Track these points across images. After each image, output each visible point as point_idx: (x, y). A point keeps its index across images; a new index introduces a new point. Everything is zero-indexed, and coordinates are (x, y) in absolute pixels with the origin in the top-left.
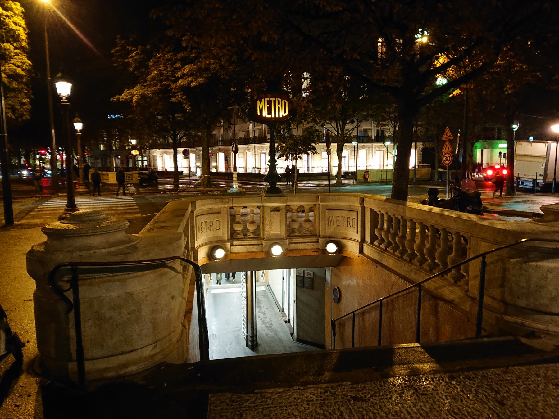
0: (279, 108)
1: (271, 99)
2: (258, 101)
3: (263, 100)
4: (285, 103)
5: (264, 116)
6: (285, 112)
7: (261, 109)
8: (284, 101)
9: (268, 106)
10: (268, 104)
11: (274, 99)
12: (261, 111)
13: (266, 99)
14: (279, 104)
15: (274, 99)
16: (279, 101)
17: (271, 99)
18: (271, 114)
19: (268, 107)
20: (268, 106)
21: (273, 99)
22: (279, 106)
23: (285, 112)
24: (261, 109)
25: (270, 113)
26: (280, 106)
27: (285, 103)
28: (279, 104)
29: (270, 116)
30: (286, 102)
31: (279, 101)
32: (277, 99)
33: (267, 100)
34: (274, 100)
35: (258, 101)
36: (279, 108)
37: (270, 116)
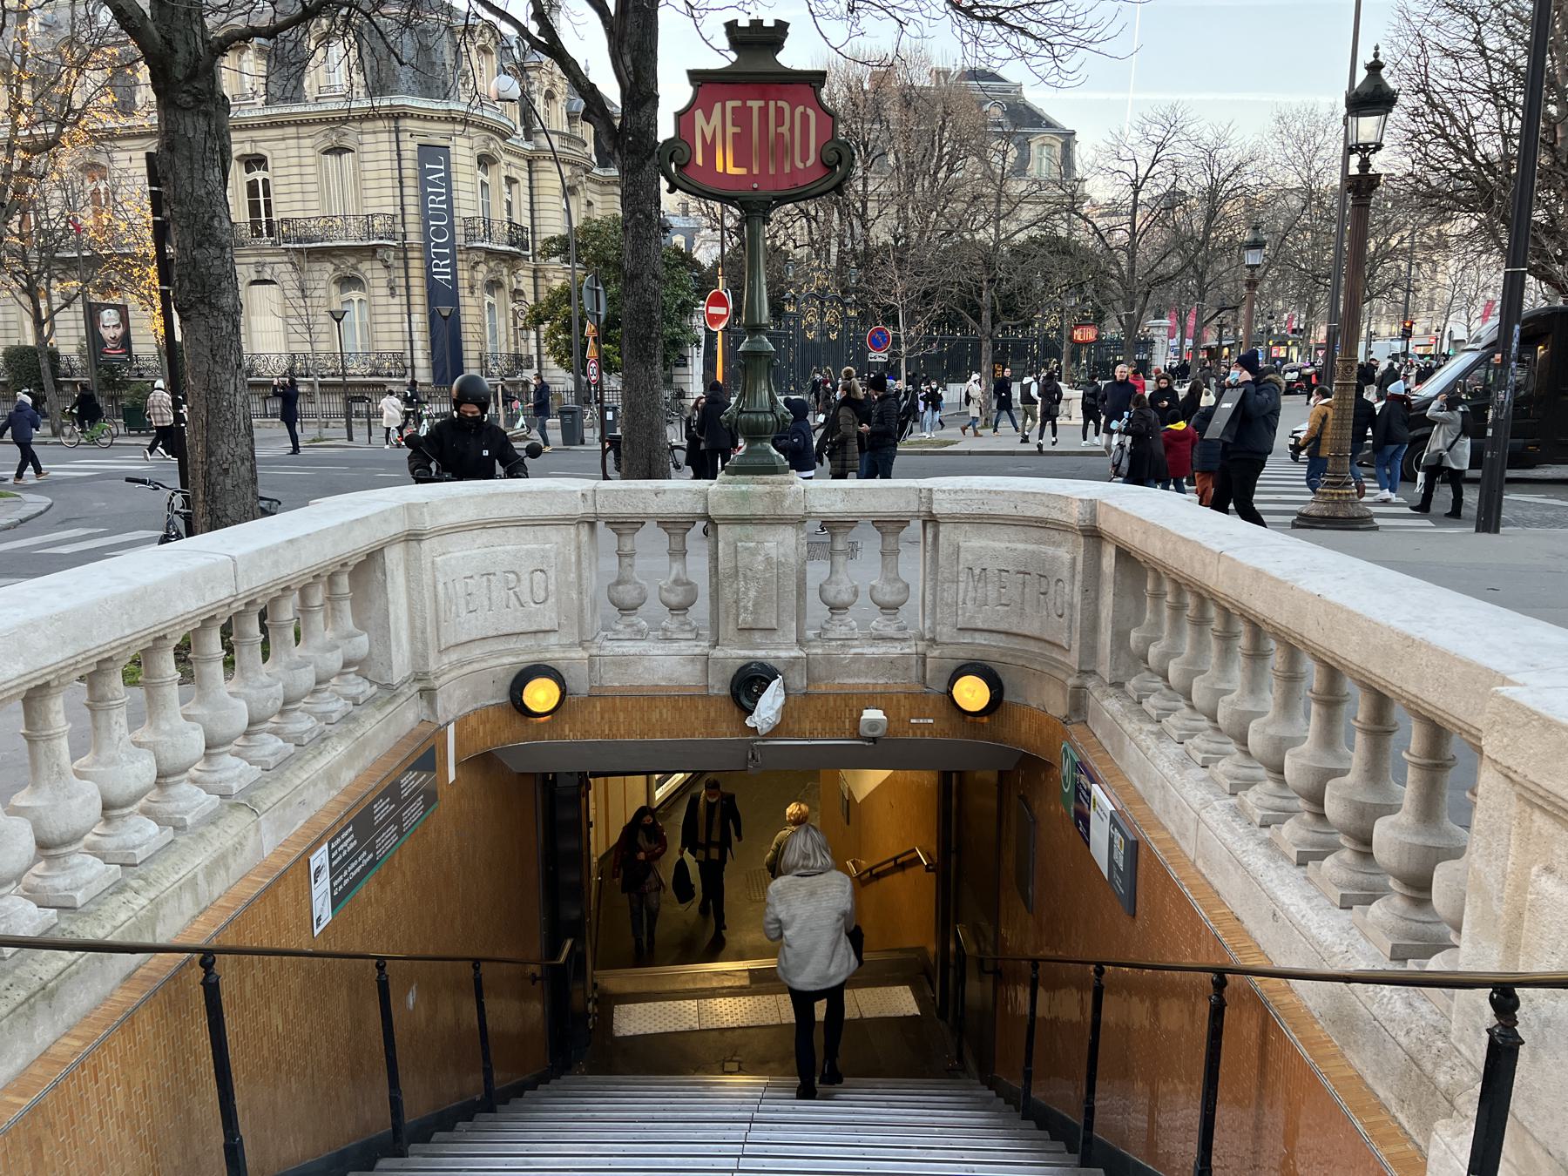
1: (749, 103)
2: (699, 114)
3: (718, 106)
4: (805, 117)
5: (720, 168)
6: (804, 158)
8: (800, 109)
9: (737, 130)
10: (734, 125)
12: (709, 151)
13: (730, 104)
15: (761, 103)
16: (780, 111)
17: (749, 103)
18: (750, 170)
20: (737, 130)
21: (755, 105)
26: (784, 129)
27: (805, 117)
28: (780, 122)
30: (811, 112)
31: (780, 111)
32: (772, 104)
33: (734, 108)
35: (699, 114)
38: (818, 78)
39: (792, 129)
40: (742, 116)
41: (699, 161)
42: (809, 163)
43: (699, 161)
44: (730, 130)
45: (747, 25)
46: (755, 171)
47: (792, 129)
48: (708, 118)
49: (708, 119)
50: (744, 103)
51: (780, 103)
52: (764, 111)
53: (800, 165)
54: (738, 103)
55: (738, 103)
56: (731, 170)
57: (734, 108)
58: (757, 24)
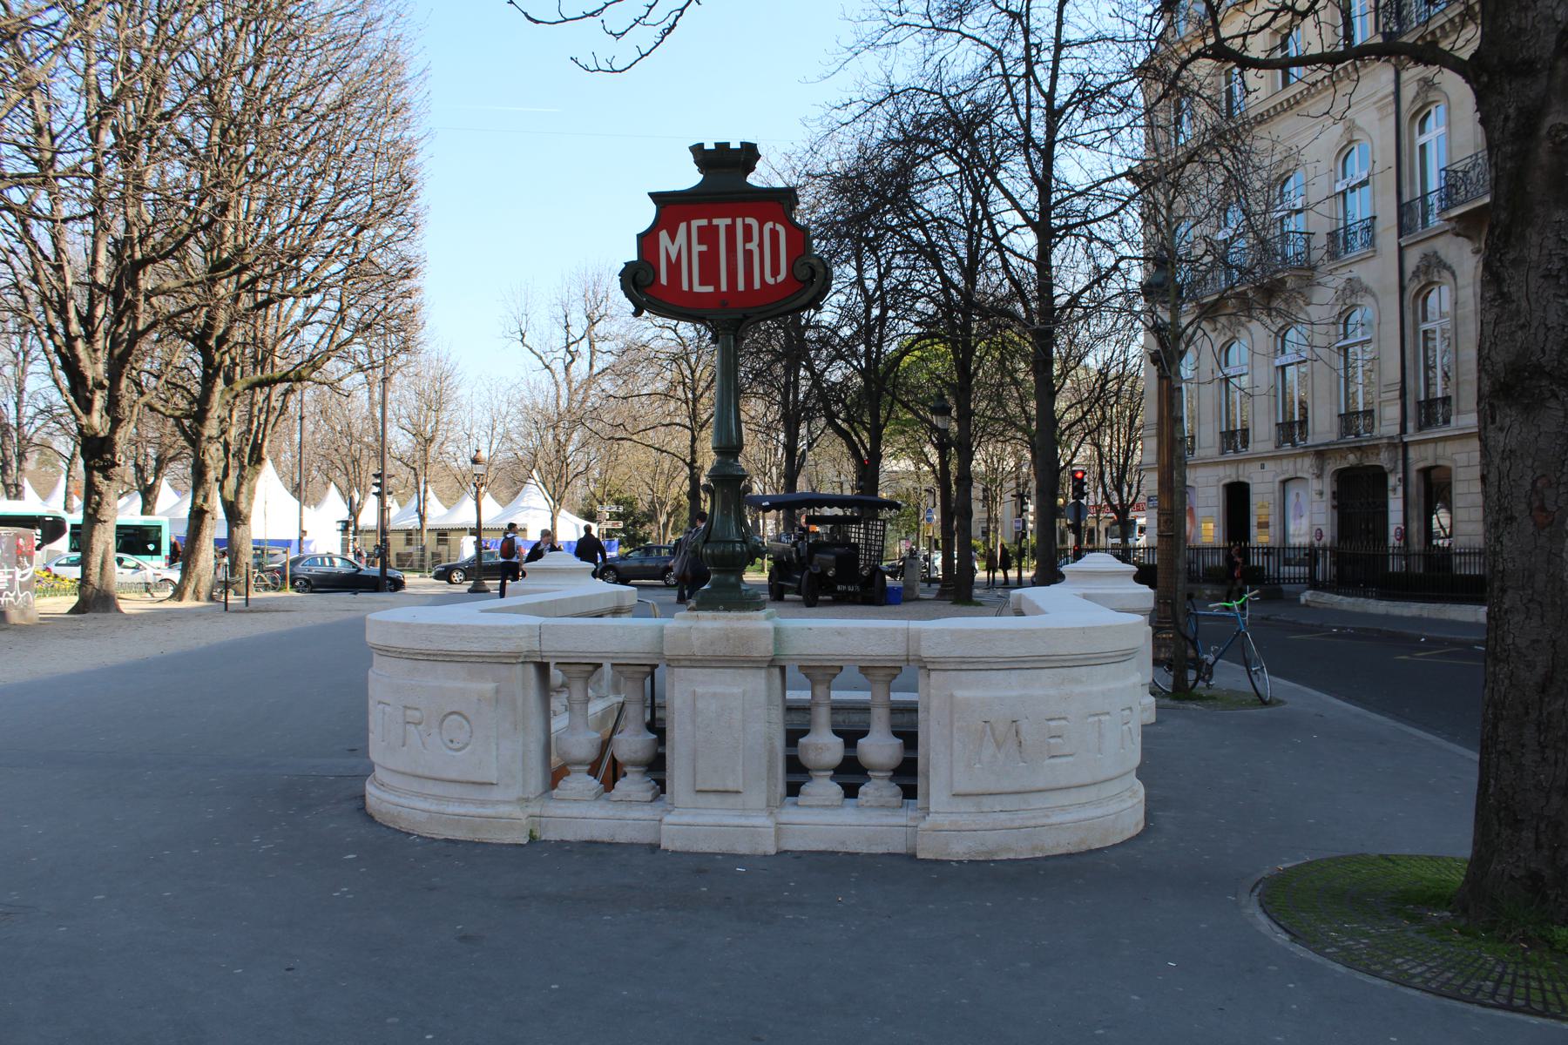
0: (748, 254)
1: (715, 221)
2: (664, 236)
3: (683, 226)
4: (774, 234)
5: (685, 287)
6: (775, 272)
7: (673, 258)
8: (769, 225)
9: (704, 248)
10: (700, 242)
11: (728, 221)
12: (674, 269)
13: (695, 224)
14: (748, 237)
15: (728, 221)
16: (748, 229)
17: (715, 221)
18: (717, 285)
20: (704, 248)
21: (722, 223)
22: (749, 246)
23: (775, 272)
24: (673, 258)
26: (753, 246)
27: (774, 234)
28: (748, 237)
29: (710, 289)
30: (780, 228)
31: (748, 229)
32: (739, 221)
33: (699, 228)
34: (727, 226)
35: (664, 236)
36: (748, 254)
37: (710, 289)
38: (787, 197)
39: (761, 245)
40: (708, 235)
41: (664, 280)
42: (781, 278)
43: (664, 280)
44: (697, 248)
45: (713, 147)
46: (724, 288)
47: (761, 245)
48: (673, 238)
49: (673, 238)
51: (749, 220)
52: (731, 230)
53: (770, 280)
54: (704, 222)
55: (704, 222)
56: (697, 288)
57: (699, 228)
58: (722, 147)
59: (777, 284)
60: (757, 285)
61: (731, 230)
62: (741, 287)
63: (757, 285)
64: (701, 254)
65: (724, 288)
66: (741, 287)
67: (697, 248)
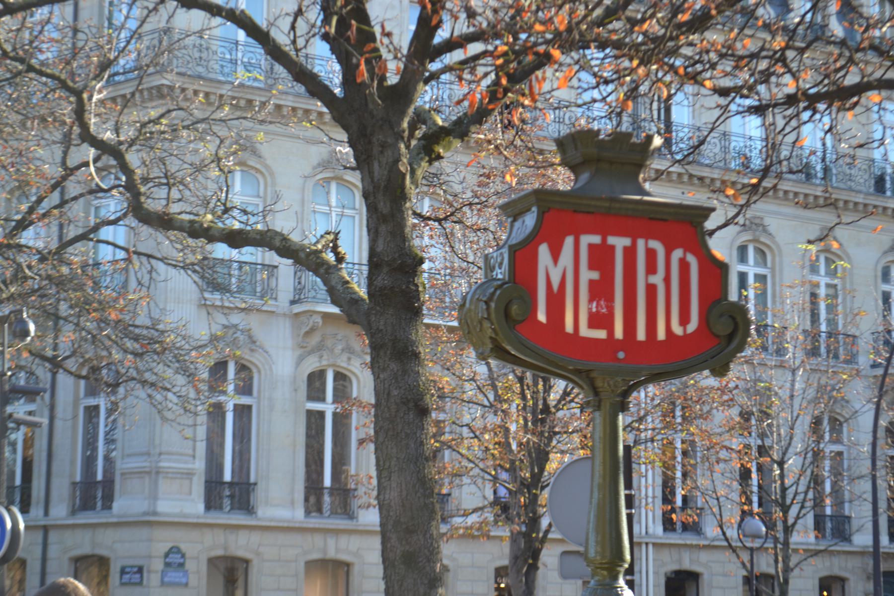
0: (651, 290)
1: (612, 240)
2: (544, 251)
3: (569, 241)
4: (684, 266)
5: (569, 327)
8: (677, 254)
9: (595, 275)
10: (591, 267)
11: (627, 242)
12: (556, 301)
14: (651, 269)
15: (627, 242)
16: (651, 255)
17: (612, 240)
19: (592, 283)
20: (595, 275)
21: (619, 243)
23: (684, 320)
25: (599, 320)
26: (657, 279)
27: (684, 266)
28: (651, 269)
29: (601, 334)
30: (692, 259)
31: (651, 255)
32: (641, 243)
33: (591, 247)
35: (544, 251)
36: (651, 290)
37: (601, 334)
41: (542, 317)
42: (692, 327)
43: (542, 317)
44: (587, 275)
47: (667, 280)
48: (555, 256)
49: (555, 256)
50: (604, 240)
52: (630, 253)
53: (677, 330)
54: (596, 239)
55: (596, 239)
56: (585, 331)
57: (591, 247)
59: (686, 336)
60: (661, 335)
61: (630, 253)
62: (641, 335)
63: (661, 335)
64: (592, 283)
65: (619, 333)
66: (641, 335)
67: (587, 275)
